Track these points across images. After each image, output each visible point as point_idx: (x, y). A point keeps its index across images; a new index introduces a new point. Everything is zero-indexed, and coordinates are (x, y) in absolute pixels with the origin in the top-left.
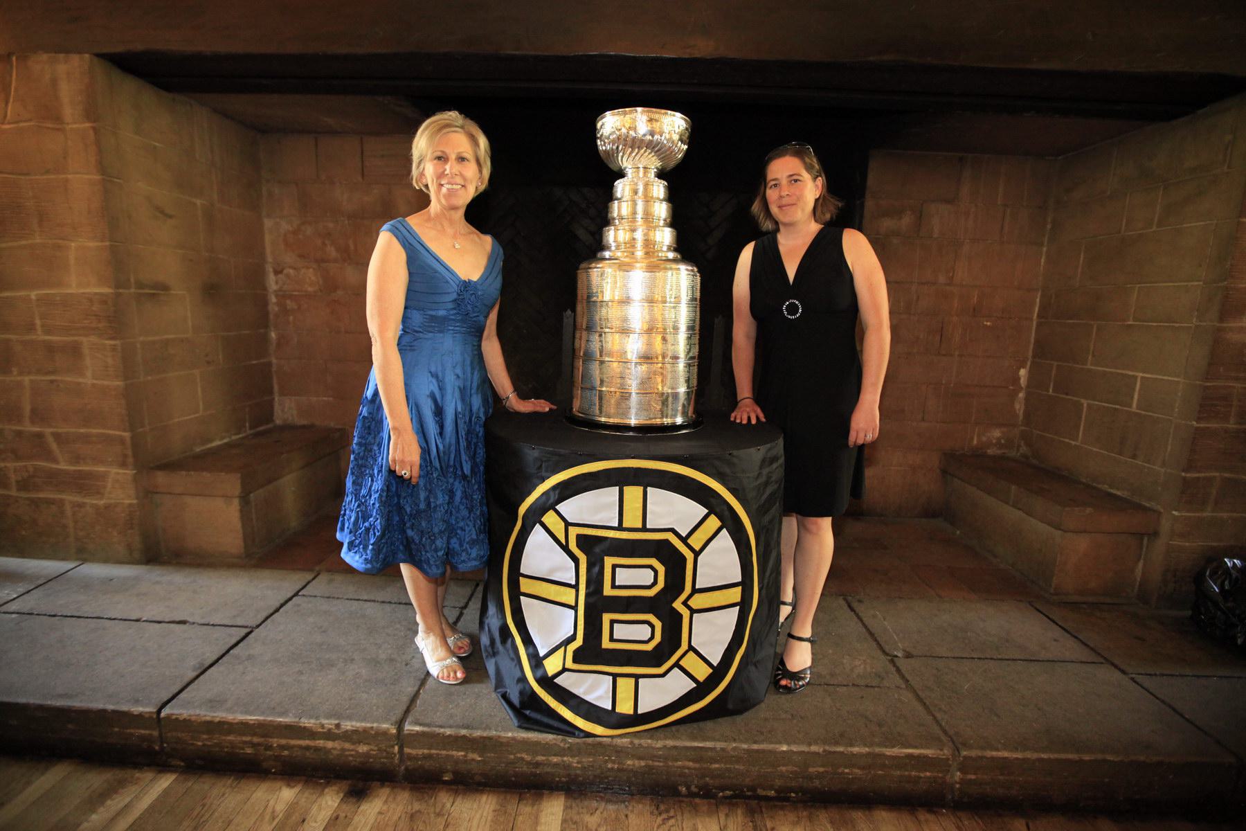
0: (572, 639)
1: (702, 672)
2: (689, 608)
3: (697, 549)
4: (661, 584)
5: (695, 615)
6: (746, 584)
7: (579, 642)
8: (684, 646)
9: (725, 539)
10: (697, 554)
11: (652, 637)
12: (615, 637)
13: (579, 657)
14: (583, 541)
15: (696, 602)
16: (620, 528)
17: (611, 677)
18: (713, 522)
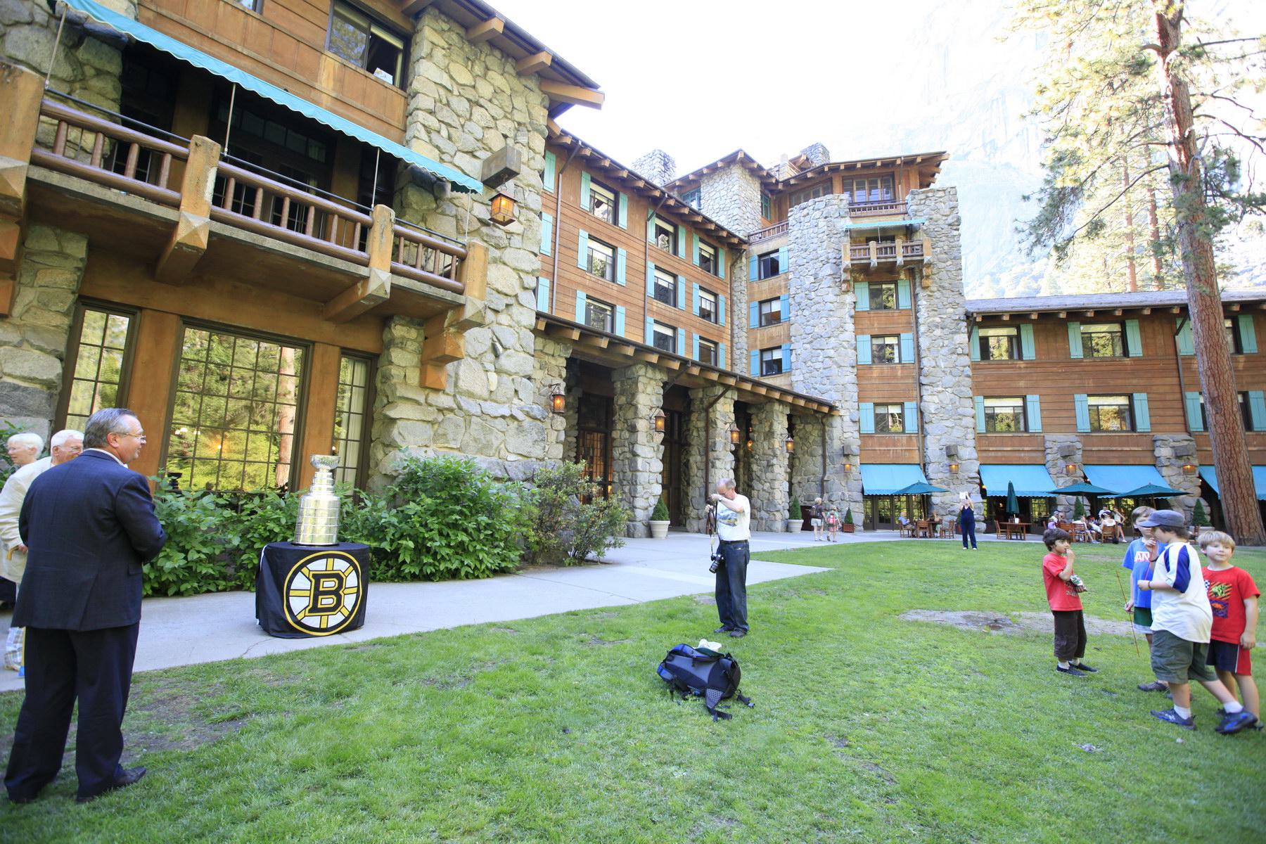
1: (346, 614)
6: (358, 587)
13: (310, 611)
14: (314, 576)
15: (347, 591)
18: (351, 568)
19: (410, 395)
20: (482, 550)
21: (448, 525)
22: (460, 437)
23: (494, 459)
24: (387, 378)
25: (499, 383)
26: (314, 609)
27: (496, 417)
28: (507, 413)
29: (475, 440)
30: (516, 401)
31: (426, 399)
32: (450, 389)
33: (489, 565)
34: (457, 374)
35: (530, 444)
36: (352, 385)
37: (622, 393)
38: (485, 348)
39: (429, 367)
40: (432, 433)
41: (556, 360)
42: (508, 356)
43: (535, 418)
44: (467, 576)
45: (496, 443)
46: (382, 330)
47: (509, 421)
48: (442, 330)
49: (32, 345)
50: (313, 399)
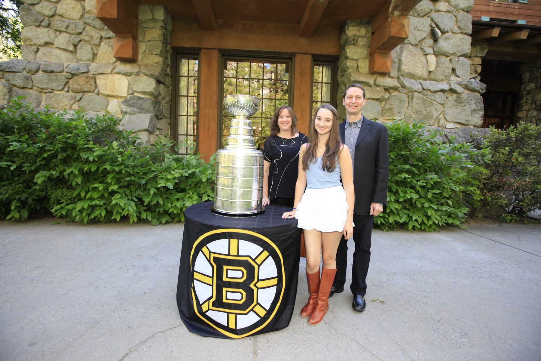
0: (211, 297)
1: (263, 313)
2: (256, 287)
3: (259, 263)
4: (245, 277)
5: (259, 290)
7: (214, 299)
8: (255, 303)
9: (270, 260)
10: (259, 266)
11: (242, 298)
12: (228, 298)
15: (260, 285)
16: (229, 255)
17: (226, 314)
18: (266, 253)
19: (362, 79)
20: (430, 207)
21: (397, 183)
22: (404, 110)
23: (435, 127)
24: (344, 71)
25: (438, 64)
26: (219, 303)
27: (436, 92)
28: (446, 87)
29: (417, 112)
30: (453, 78)
31: (375, 81)
32: (394, 73)
33: (437, 222)
34: (400, 60)
35: (469, 113)
36: (322, 83)
37: (530, 81)
38: (424, 35)
39: (377, 56)
40: (381, 109)
41: (473, 60)
42: (446, 38)
43: (473, 90)
44: (414, 228)
45: (435, 114)
46: (340, 37)
47: (448, 95)
48: (388, 17)
49: (143, 73)
50: (297, 93)
